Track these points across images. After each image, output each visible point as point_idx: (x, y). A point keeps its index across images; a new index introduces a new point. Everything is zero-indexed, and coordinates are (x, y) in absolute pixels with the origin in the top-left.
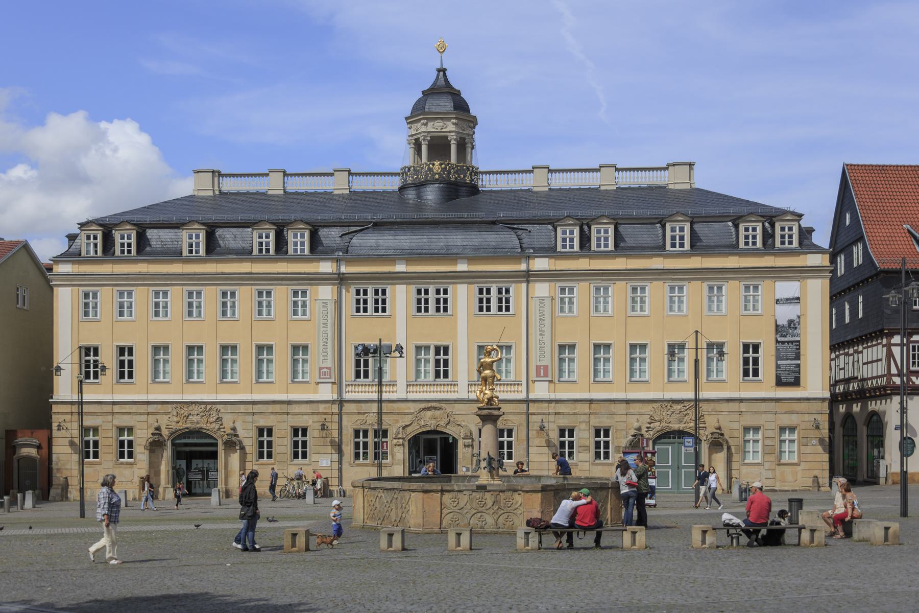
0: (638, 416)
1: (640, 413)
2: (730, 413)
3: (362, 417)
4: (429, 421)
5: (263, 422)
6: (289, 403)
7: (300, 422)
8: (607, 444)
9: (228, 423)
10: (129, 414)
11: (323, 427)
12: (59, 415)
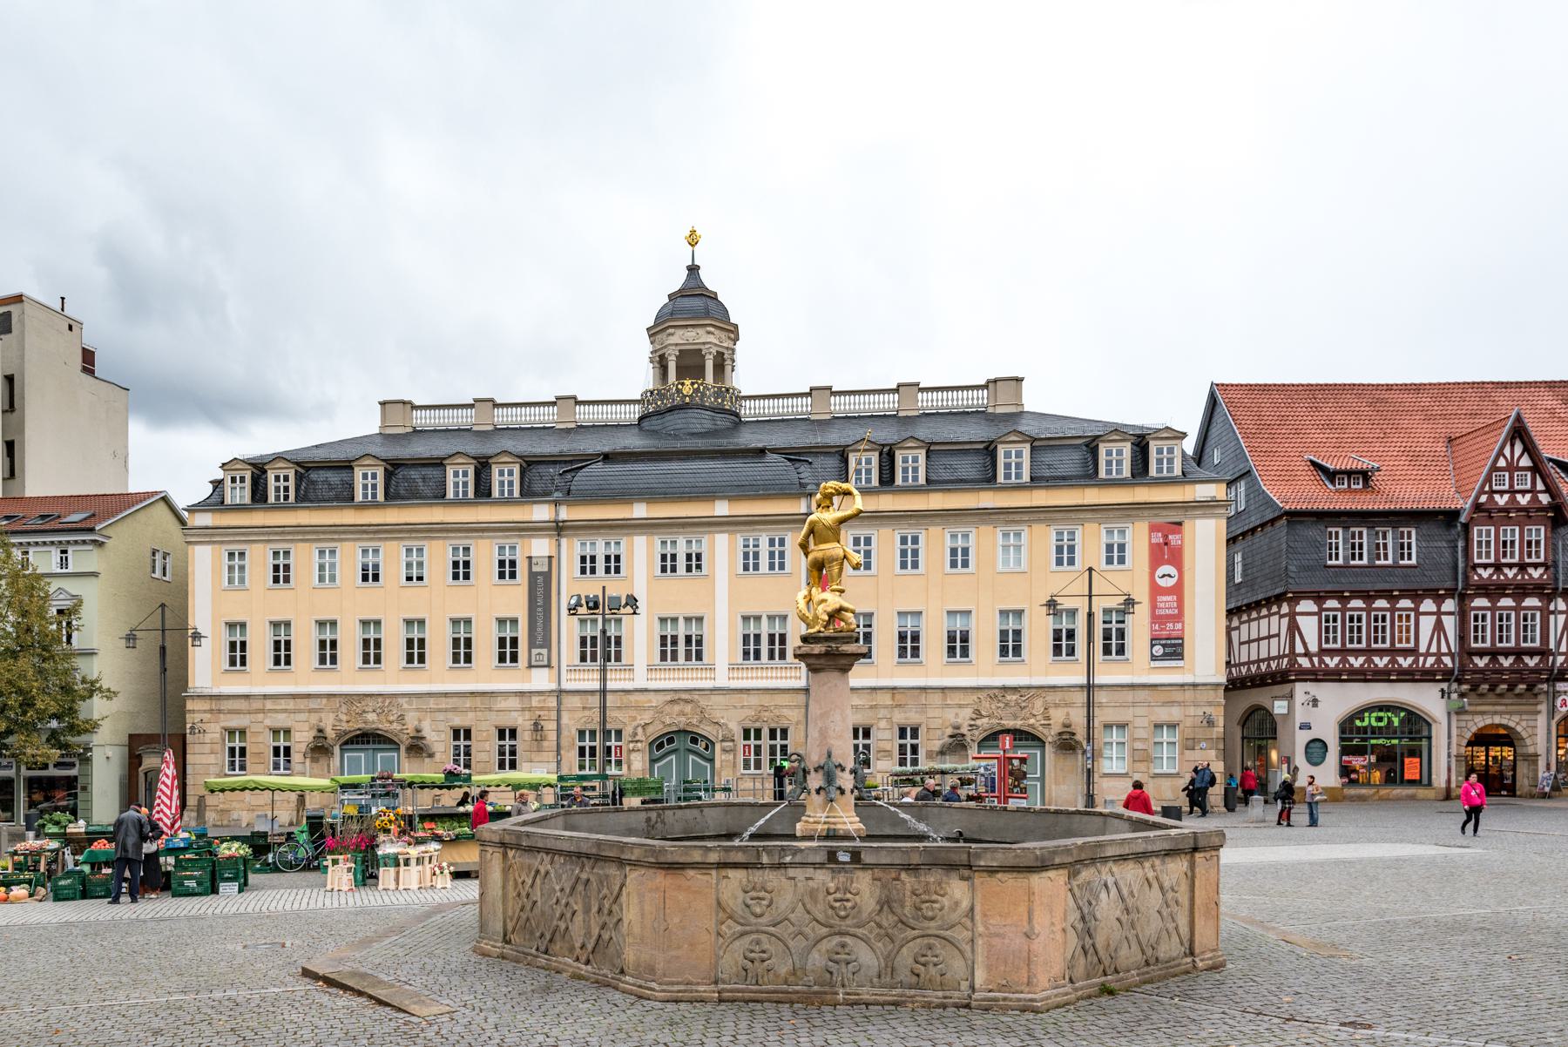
1: (960, 706)
3: (587, 713)
4: (676, 718)
5: (459, 721)
6: (492, 694)
7: (507, 721)
8: (915, 749)
9: (411, 722)
10: (285, 711)
11: (537, 727)
12: (196, 712)
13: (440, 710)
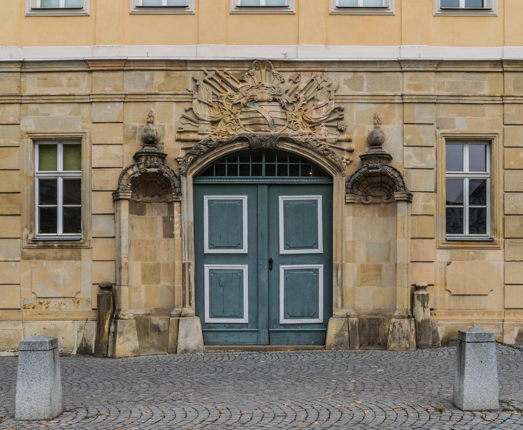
13: (424, 101)
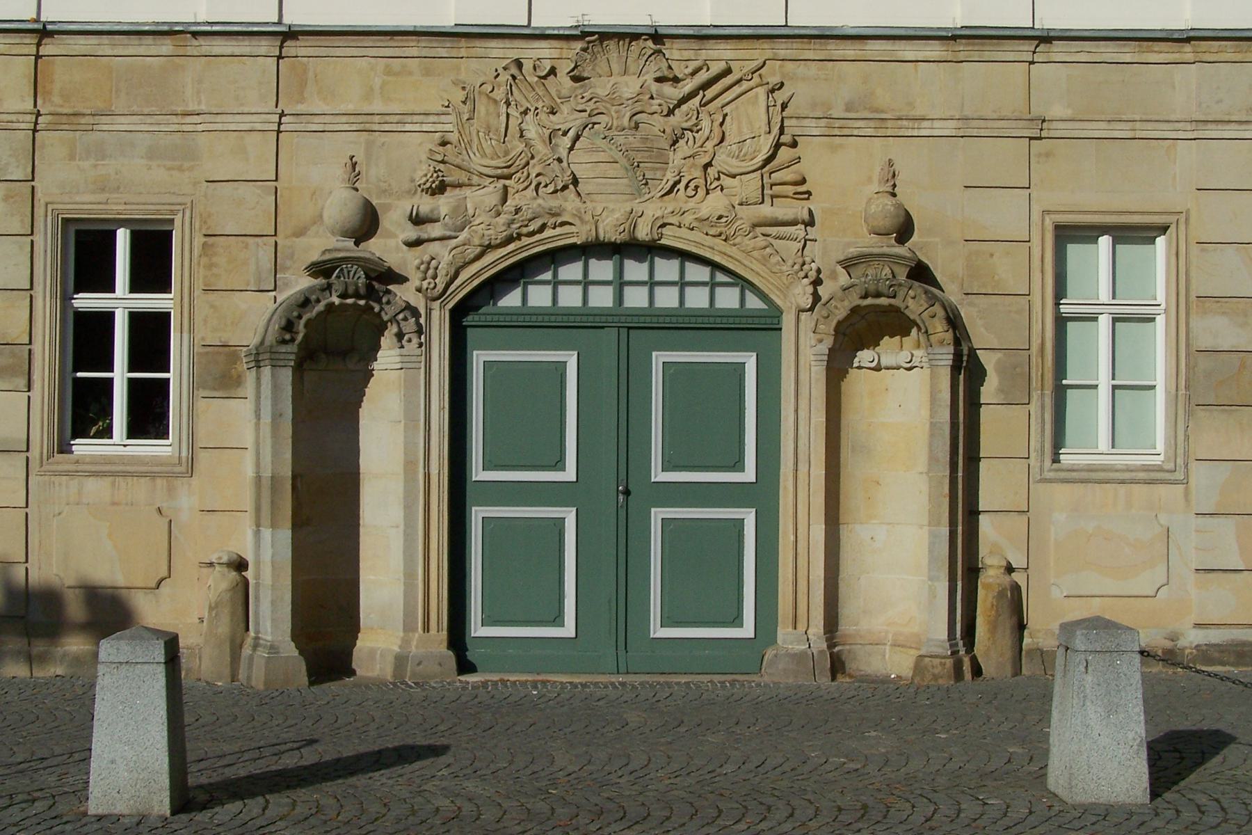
0: (355, 145)
2: (969, 127)
8: (151, 336)
